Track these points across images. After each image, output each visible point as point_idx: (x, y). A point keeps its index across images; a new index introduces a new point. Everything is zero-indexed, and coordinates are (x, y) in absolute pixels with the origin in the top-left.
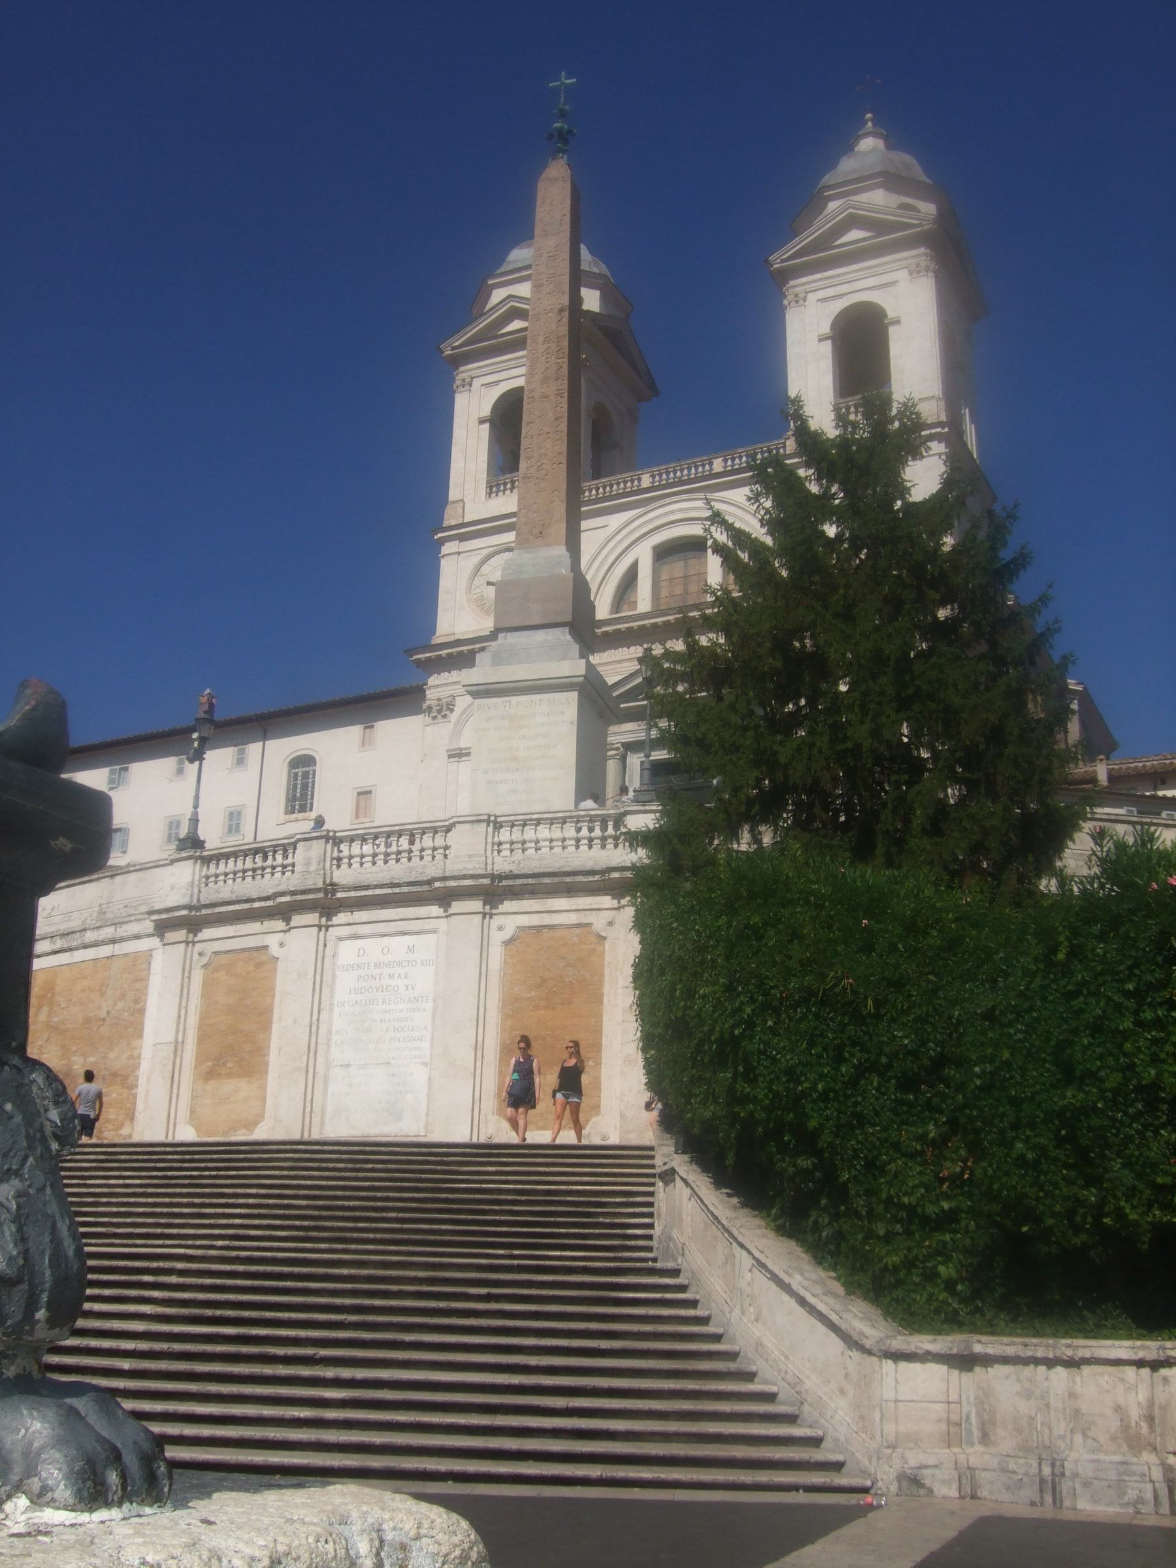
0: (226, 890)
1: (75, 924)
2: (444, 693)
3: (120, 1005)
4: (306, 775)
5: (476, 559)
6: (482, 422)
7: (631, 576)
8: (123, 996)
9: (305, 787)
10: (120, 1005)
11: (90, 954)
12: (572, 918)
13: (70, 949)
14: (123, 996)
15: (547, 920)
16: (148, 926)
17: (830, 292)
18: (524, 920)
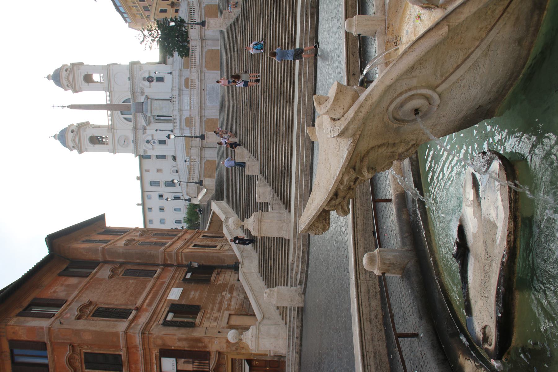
0: (178, 127)
2: (142, 151)
4: (153, 183)
9: (155, 183)
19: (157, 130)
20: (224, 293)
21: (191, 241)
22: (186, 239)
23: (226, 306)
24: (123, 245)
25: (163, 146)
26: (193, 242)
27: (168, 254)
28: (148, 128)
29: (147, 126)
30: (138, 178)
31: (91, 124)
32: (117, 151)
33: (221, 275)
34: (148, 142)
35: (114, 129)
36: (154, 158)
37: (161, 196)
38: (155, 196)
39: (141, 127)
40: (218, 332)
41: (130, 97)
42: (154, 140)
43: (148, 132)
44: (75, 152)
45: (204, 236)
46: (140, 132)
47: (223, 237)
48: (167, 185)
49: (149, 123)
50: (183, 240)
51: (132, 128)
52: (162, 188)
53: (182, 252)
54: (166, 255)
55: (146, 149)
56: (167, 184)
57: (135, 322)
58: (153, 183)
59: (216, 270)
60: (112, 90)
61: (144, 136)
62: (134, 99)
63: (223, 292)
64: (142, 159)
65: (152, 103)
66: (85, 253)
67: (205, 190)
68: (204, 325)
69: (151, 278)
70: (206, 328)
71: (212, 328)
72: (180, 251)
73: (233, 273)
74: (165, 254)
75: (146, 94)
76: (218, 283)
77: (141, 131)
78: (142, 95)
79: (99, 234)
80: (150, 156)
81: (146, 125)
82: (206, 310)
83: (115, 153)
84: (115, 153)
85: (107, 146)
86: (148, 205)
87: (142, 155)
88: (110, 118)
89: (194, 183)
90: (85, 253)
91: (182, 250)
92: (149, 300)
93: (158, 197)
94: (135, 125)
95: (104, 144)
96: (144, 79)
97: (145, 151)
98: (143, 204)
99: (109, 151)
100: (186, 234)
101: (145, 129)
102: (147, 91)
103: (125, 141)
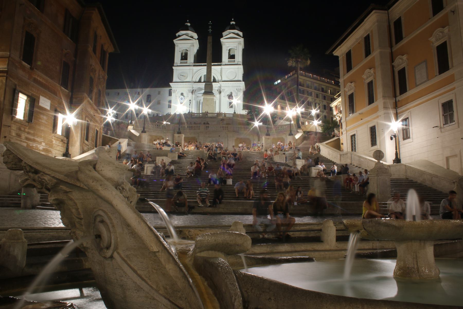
19: (190, 100)
20: (43, 144)
23: (31, 145)
33: (61, 143)
40: (6, 136)
42: (183, 99)
45: (97, 132)
57: (19, 67)
59: (65, 139)
63: (44, 143)
67: (137, 134)
68: (13, 125)
69: (60, 84)
70: (9, 126)
71: (10, 132)
73: (62, 153)
76: (53, 139)
82: (28, 127)
87: (171, 90)
89: (144, 126)
92: (40, 81)
96: (231, 93)
97: (175, 91)
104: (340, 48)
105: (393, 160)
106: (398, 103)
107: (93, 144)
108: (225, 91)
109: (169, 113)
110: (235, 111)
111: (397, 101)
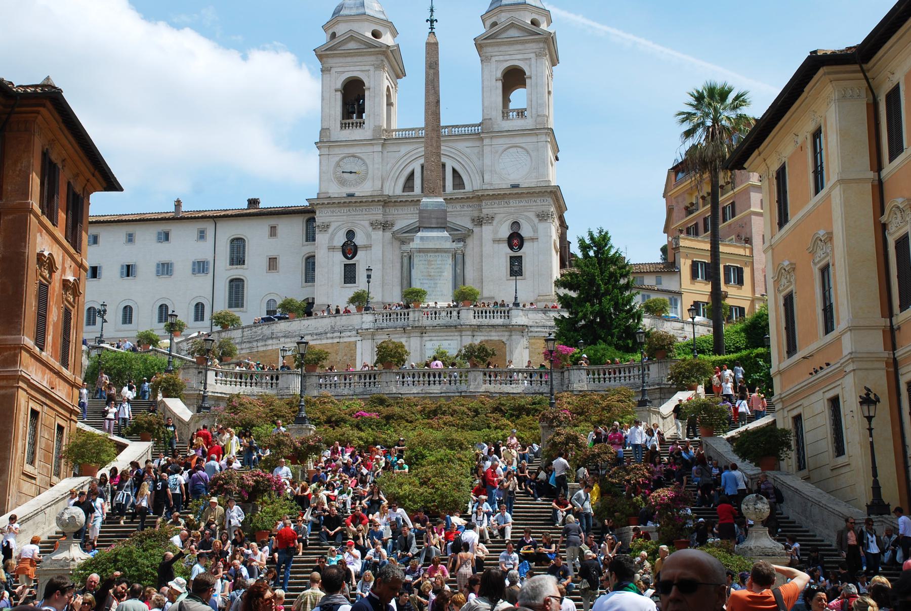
1: (321, 330)
2: (326, 220)
3: (345, 358)
4: (238, 247)
5: (337, 159)
6: (336, 91)
7: (411, 176)
8: (346, 355)
9: (238, 252)
10: (345, 358)
11: (330, 341)
12: (496, 338)
13: (321, 339)
14: (346, 355)
15: (490, 338)
16: (354, 333)
17: (501, 58)
18: (483, 338)
21: (48, 402)
22: (52, 388)
24: (38, 251)
25: (338, 272)
26: (45, 408)
27: (16, 356)
28: (388, 234)
29: (393, 234)
30: (253, 202)
31: (398, 80)
32: (325, 151)
34: (350, 234)
35: (383, 145)
36: (308, 249)
37: (200, 267)
38: (204, 251)
39: (390, 218)
41: (468, 187)
43: (378, 235)
44: (322, 39)
45: (60, 428)
46: (377, 214)
47: (58, 474)
48: (234, 283)
49: (402, 238)
50: (51, 383)
51: (386, 193)
52: (225, 272)
53: (18, 387)
54: (12, 352)
55: (331, 230)
56: (236, 287)
58: (238, 247)
60: (486, 141)
61: (366, 224)
62: (462, 198)
64: (306, 218)
65: (446, 252)
66: (18, 169)
72: (21, 384)
74: (15, 348)
75: (476, 230)
77: (380, 218)
78: (473, 220)
79: (69, 184)
80: (314, 240)
81: (395, 228)
83: (319, 145)
84: (319, 148)
85: (339, 125)
86: (176, 231)
87: (314, 219)
88: (413, 134)
90: (18, 169)
91: (24, 386)
93: (200, 257)
94: (395, 202)
95: (343, 119)
96: (516, 224)
97: (326, 227)
98: (178, 218)
99: (324, 131)
100: (67, 386)
101: (385, 226)
102: (487, 231)
103: (351, 172)
104: (760, 154)
105: (867, 506)
106: (897, 333)
107: (48, 469)
108: (495, 223)
109: (308, 299)
110: (516, 298)
111: (895, 327)
